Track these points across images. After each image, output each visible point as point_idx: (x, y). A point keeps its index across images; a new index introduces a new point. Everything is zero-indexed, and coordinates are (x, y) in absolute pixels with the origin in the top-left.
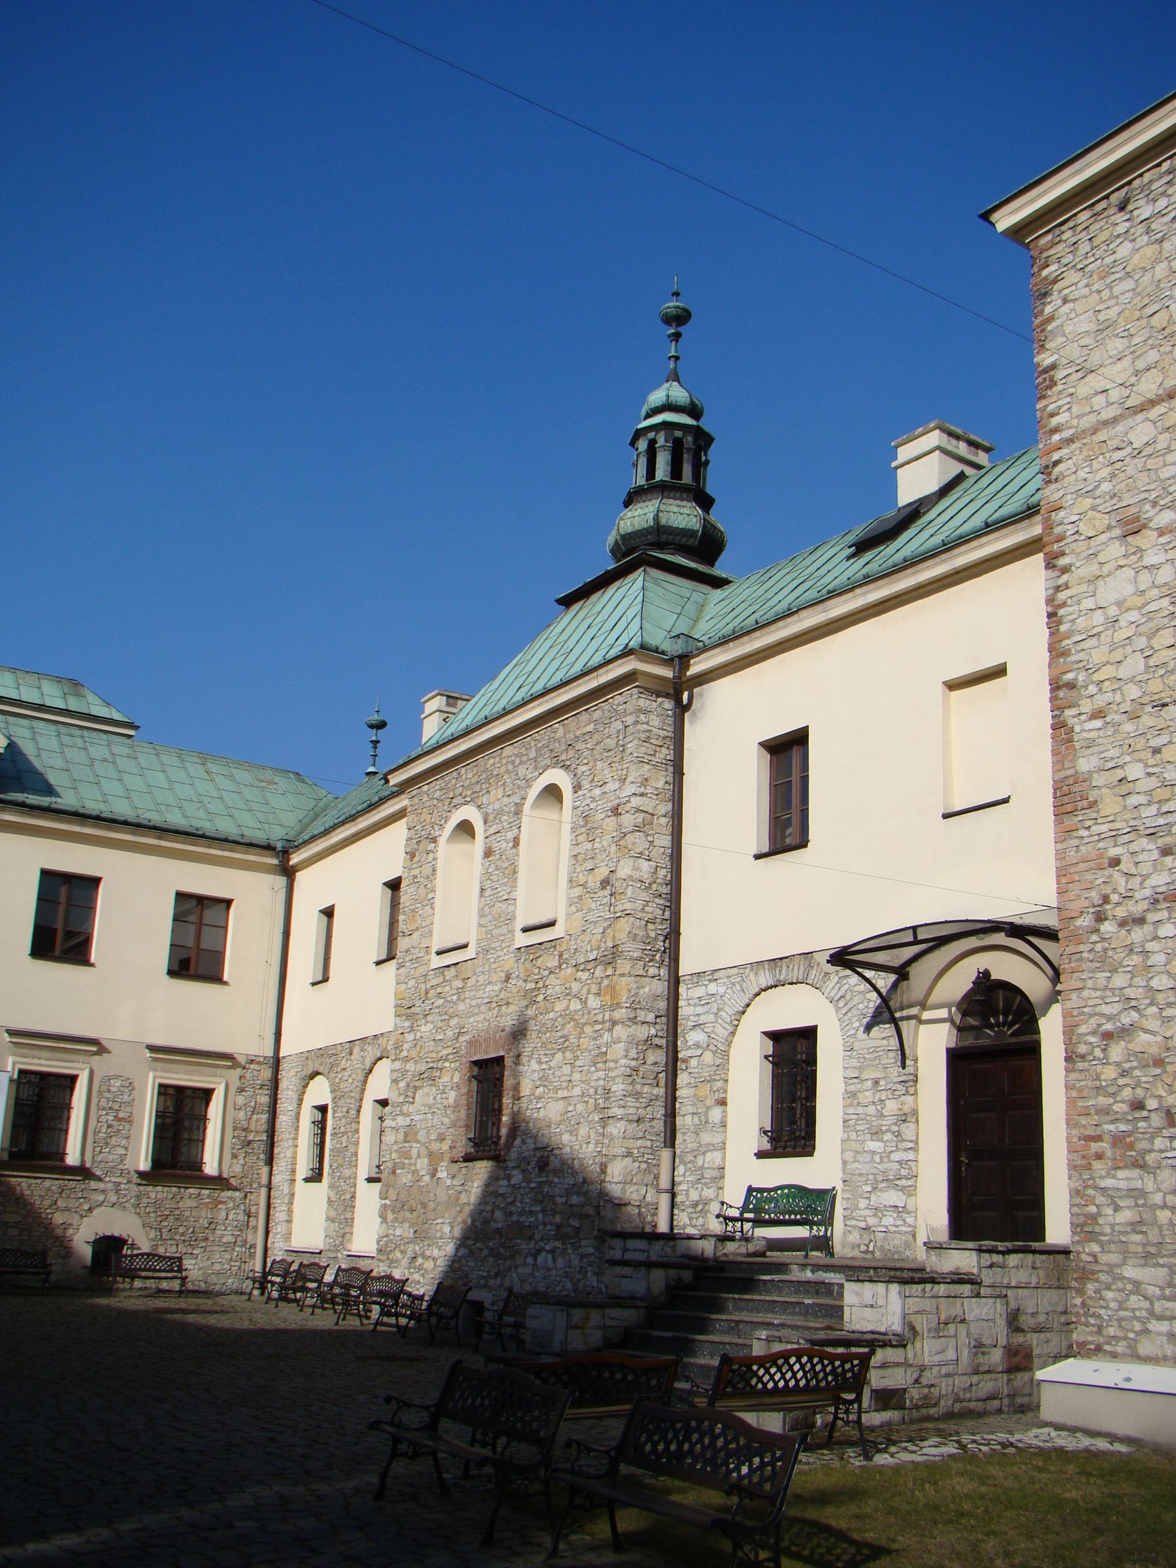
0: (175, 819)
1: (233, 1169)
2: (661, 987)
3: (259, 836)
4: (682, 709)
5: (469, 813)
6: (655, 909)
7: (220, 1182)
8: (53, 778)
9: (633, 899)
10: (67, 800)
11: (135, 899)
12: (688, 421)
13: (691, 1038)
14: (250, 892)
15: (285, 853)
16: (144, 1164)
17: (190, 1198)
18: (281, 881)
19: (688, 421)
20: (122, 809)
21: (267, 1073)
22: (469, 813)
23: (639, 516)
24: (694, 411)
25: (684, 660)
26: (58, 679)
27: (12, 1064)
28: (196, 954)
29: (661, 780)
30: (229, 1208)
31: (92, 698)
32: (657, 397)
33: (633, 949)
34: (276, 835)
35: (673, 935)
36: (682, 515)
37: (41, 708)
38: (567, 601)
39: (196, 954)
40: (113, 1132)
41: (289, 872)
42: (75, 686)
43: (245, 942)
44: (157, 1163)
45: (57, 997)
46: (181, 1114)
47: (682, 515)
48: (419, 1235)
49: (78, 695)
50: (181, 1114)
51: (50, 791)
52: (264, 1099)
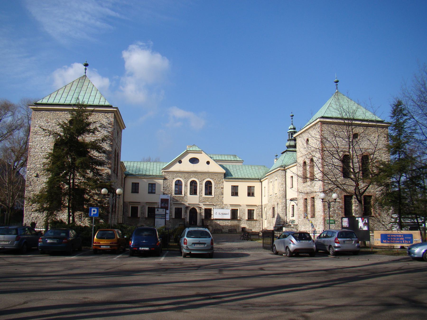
0: (247, 177)
1: (258, 219)
2: (285, 201)
3: (257, 178)
4: (286, 172)
5: (271, 180)
6: (284, 193)
7: (256, 220)
8: (232, 173)
9: (281, 192)
10: (234, 177)
11: (243, 187)
12: (293, 130)
13: (287, 206)
14: (256, 185)
15: (260, 180)
16: (247, 219)
17: (253, 222)
18: (260, 183)
19: (293, 130)
20: (240, 177)
21: (261, 207)
22: (271, 180)
23: (288, 144)
24: (294, 129)
25: (285, 167)
26: (233, 155)
27: (231, 208)
28: (251, 193)
29: (284, 180)
30: (257, 224)
31: (237, 158)
32: (290, 128)
33: (281, 197)
34: (260, 177)
35: (286, 195)
36: (292, 143)
37: (231, 161)
38: (282, 153)
39: (251, 193)
40: (243, 215)
41: (261, 182)
42: (235, 156)
43: (257, 192)
44: (248, 218)
45: (235, 200)
46: (251, 213)
47: (292, 143)
48: (270, 225)
49: (236, 157)
50: (251, 213)
51: (231, 175)
52: (261, 210)
